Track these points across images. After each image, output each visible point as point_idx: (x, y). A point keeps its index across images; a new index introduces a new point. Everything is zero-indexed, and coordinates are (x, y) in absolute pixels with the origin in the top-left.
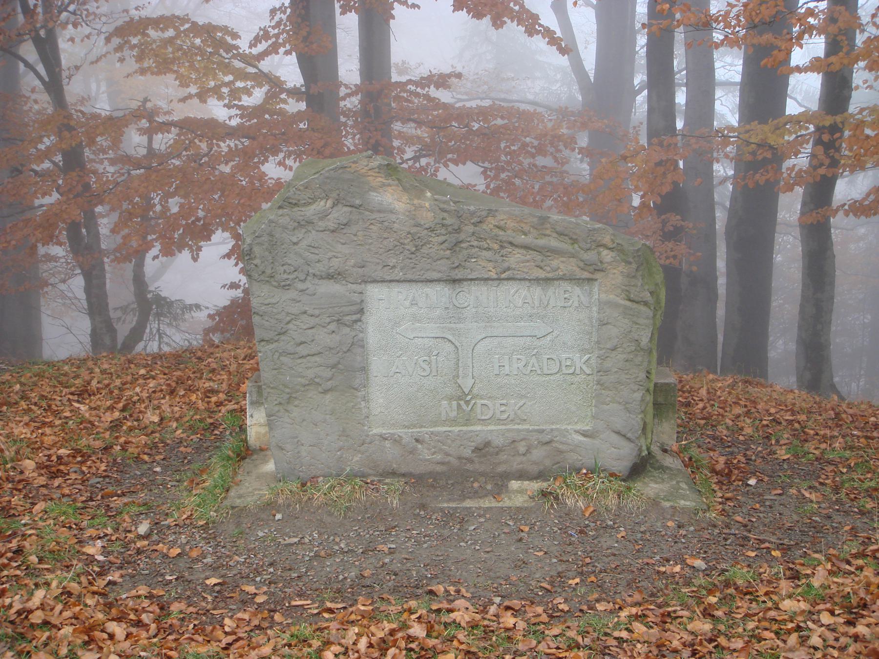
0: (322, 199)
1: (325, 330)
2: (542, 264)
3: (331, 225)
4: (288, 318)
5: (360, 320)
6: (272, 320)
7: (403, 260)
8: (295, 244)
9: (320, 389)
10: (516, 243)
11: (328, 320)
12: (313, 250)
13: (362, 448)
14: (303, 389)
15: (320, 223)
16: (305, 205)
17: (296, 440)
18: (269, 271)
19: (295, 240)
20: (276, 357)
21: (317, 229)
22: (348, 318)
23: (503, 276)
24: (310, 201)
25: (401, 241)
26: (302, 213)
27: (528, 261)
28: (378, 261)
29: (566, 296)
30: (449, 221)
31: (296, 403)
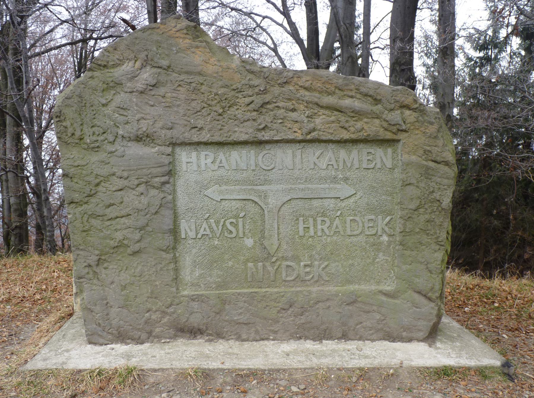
0: (130, 60)
1: (134, 192)
2: (347, 125)
3: (140, 86)
4: (98, 181)
5: (168, 183)
6: (81, 182)
7: (211, 121)
8: (103, 105)
9: (129, 251)
10: (321, 104)
11: (136, 182)
12: (122, 112)
13: (171, 310)
14: (112, 251)
15: (129, 85)
16: (114, 66)
17: (105, 302)
18: (78, 133)
19: (104, 101)
20: (85, 219)
21: (126, 90)
22: (157, 179)
23: (309, 137)
24: (118, 62)
25: (209, 102)
26: (111, 74)
27: (333, 122)
28: (186, 123)
29: (369, 158)
30: (256, 82)
31: (105, 265)
